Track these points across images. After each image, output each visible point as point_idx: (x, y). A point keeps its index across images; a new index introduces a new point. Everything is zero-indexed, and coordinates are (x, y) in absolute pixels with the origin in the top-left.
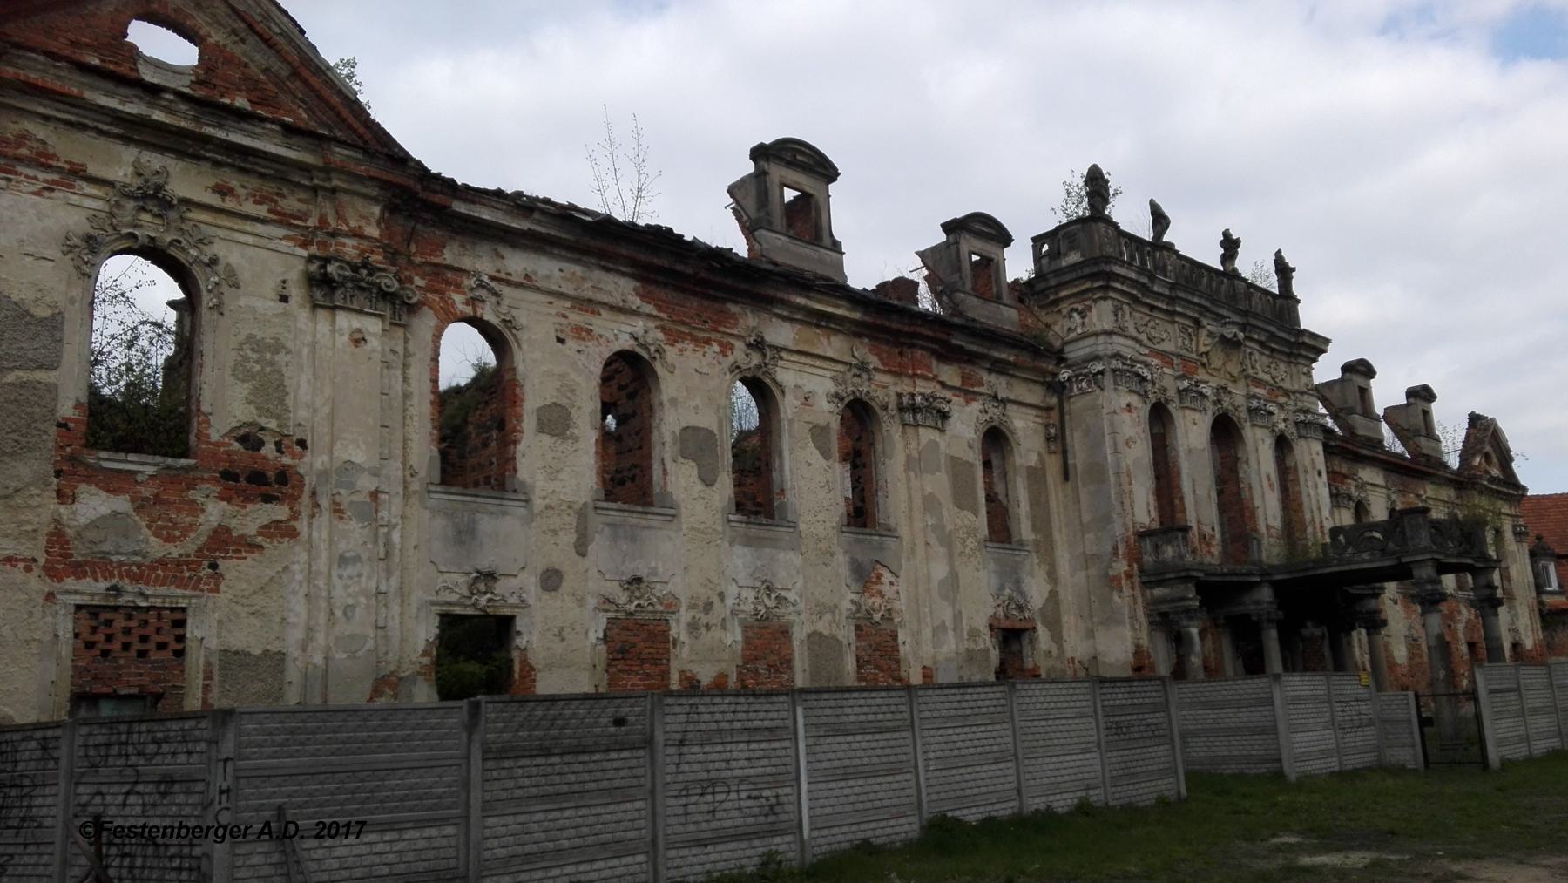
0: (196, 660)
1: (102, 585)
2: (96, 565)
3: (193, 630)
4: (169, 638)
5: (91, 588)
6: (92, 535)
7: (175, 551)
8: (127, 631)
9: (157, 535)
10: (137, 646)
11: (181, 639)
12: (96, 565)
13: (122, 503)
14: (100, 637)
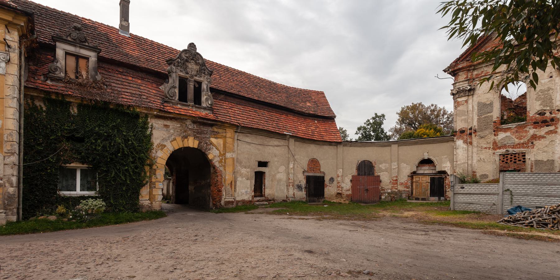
0: (528, 163)
1: (505, 150)
2: (504, 146)
3: (527, 157)
4: (521, 158)
5: (503, 151)
6: (502, 141)
7: (522, 141)
8: (511, 158)
9: (517, 139)
10: (514, 161)
11: (525, 159)
12: (504, 146)
13: (508, 134)
14: (505, 160)
